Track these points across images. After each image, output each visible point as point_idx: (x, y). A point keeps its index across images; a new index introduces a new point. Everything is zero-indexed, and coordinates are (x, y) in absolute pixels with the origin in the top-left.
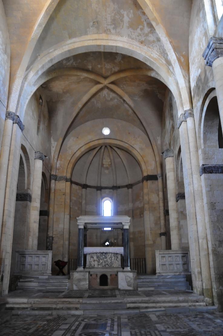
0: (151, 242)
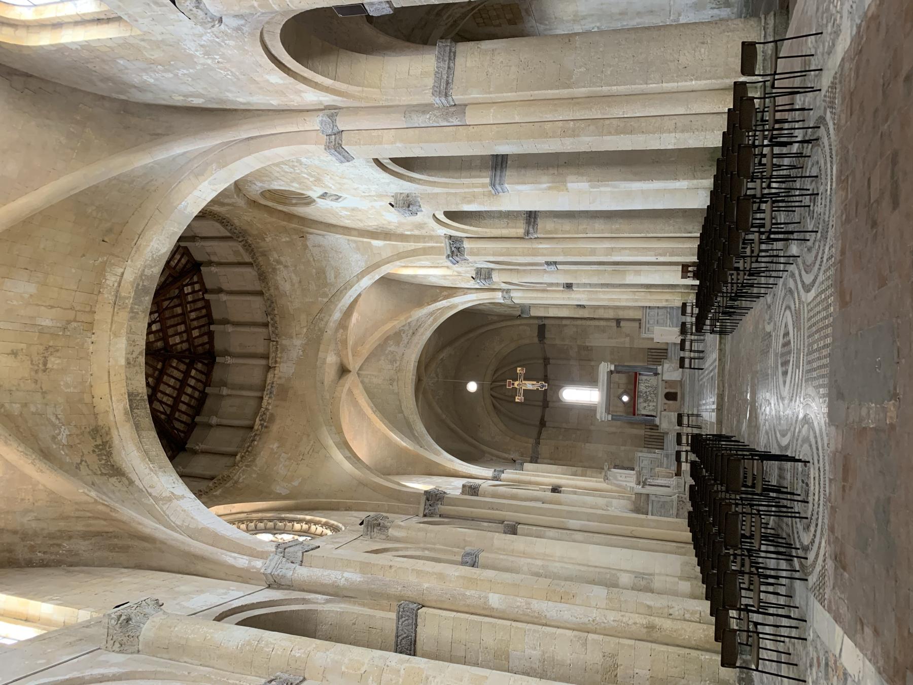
0: (628, 339)
